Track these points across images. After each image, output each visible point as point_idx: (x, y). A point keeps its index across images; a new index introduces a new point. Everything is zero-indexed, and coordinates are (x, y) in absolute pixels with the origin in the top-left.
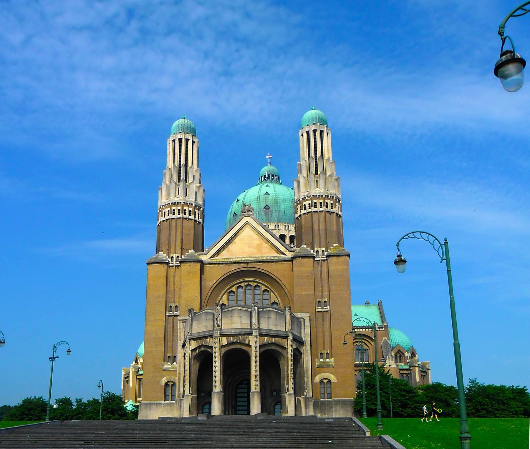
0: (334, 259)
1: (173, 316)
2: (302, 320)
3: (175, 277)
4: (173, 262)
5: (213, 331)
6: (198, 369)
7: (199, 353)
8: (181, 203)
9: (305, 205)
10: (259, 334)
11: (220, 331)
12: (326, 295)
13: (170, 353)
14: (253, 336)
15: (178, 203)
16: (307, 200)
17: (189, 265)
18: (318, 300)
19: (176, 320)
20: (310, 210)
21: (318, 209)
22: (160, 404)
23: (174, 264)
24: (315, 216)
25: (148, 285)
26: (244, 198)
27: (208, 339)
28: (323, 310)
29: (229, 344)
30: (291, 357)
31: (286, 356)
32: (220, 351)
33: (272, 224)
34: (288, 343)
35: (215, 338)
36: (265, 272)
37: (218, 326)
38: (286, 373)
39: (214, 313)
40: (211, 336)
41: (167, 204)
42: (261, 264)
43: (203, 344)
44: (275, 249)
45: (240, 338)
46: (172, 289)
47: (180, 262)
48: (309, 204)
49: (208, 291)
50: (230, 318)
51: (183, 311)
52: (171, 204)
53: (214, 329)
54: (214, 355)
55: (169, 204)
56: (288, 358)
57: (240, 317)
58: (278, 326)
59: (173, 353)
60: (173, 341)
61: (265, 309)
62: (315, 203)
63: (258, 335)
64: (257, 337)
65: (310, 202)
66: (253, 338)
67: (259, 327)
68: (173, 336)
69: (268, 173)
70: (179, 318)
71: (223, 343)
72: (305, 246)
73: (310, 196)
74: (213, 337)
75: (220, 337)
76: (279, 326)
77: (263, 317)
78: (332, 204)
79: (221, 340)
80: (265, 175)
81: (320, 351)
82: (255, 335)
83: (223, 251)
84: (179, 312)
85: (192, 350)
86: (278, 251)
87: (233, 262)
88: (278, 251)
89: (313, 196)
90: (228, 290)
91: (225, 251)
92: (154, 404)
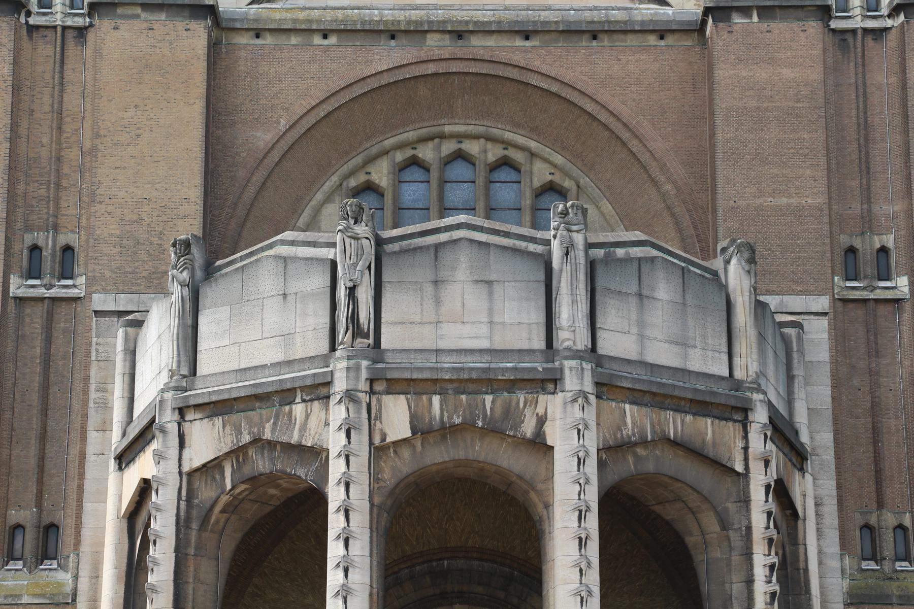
1: (46, 301)
2: (791, 331)
3: (62, 90)
4: (50, 8)
5: (325, 359)
6: (221, 582)
7: (233, 488)
10: (598, 384)
11: (375, 361)
12: (887, 216)
13: (25, 509)
14: (560, 396)
17: (145, 25)
18: (845, 240)
19: (62, 325)
23: (58, 20)
27: (298, 409)
28: (872, 296)
30: (767, 528)
31: (737, 521)
32: (375, 477)
34: (746, 449)
35: (340, 402)
36: (554, 88)
37: (357, 332)
39: (334, 264)
42: (533, 47)
43: (268, 435)
45: (488, 406)
46: (44, 152)
49: (242, 173)
50: (429, 289)
51: (108, 274)
53: (333, 348)
54: (335, 496)
56: (749, 529)
57: (483, 290)
58: (695, 347)
59: (39, 504)
60: (43, 439)
61: (620, 252)
63: (589, 387)
64: (586, 398)
66: (565, 403)
67: (594, 349)
68: (45, 410)
70: (101, 302)
71: (388, 431)
74: (328, 397)
75: (372, 392)
76: (697, 350)
77: (613, 292)
79: (380, 410)
81: (857, 515)
82: (577, 388)
84: (81, 280)
85: (191, 474)
87: (382, 28)
90: (352, 173)
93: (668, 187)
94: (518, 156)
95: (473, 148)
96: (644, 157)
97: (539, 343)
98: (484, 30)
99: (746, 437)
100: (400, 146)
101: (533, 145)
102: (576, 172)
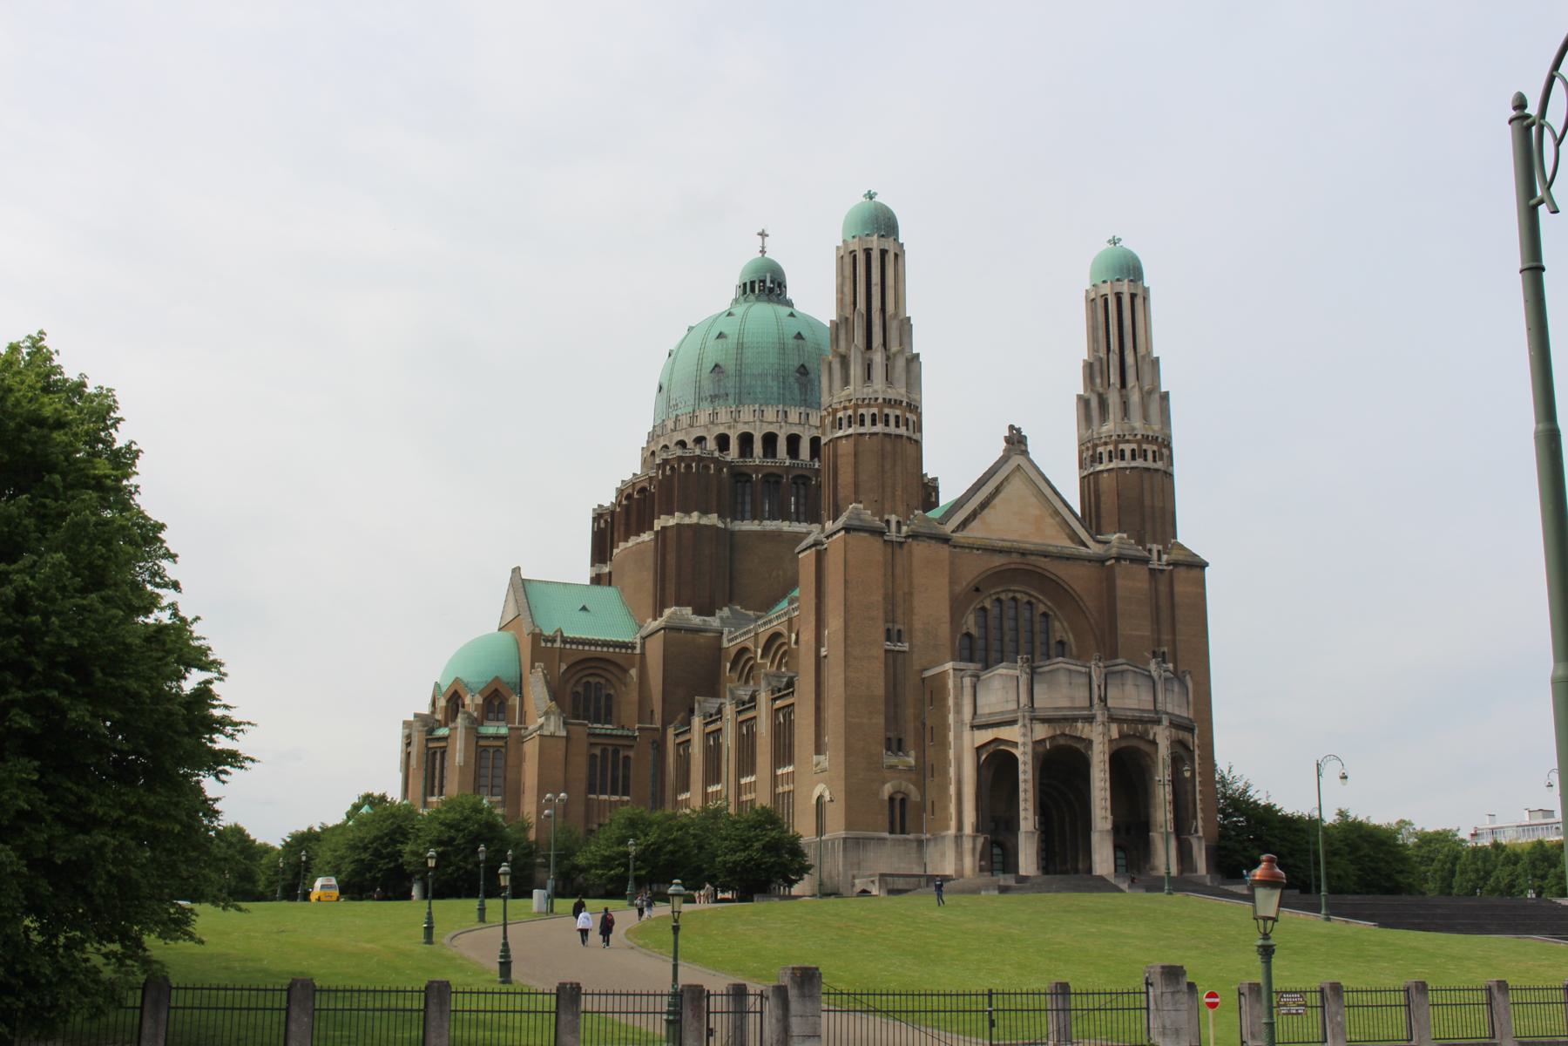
0: (1181, 573)
8: (901, 402)
9: (1122, 451)
14: (1161, 727)
15: (895, 401)
16: (1128, 441)
20: (1134, 464)
21: (1150, 464)
22: (884, 839)
24: (1146, 475)
25: (847, 578)
26: (741, 333)
27: (1080, 725)
29: (1122, 736)
33: (815, 413)
34: (1193, 742)
36: (1055, 578)
38: (1190, 798)
40: (1090, 719)
41: (870, 399)
43: (1067, 732)
44: (1067, 531)
47: (908, 537)
48: (1133, 450)
52: (880, 401)
55: (876, 399)
62: (1145, 451)
65: (1134, 446)
69: (771, 277)
72: (1125, 536)
73: (1136, 435)
74: (1091, 722)
78: (1154, 452)
80: (762, 278)
83: (973, 520)
86: (1074, 537)
88: (1074, 537)
89: (1143, 435)
90: (979, 603)
91: (976, 521)
92: (873, 839)
93: (1092, 621)
94: (1034, 601)
95: (1018, 596)
96: (1084, 608)
97: (1153, 708)
98: (1032, 553)
99: (1193, 738)
100: (994, 594)
101: (1041, 597)
102: (1055, 609)
